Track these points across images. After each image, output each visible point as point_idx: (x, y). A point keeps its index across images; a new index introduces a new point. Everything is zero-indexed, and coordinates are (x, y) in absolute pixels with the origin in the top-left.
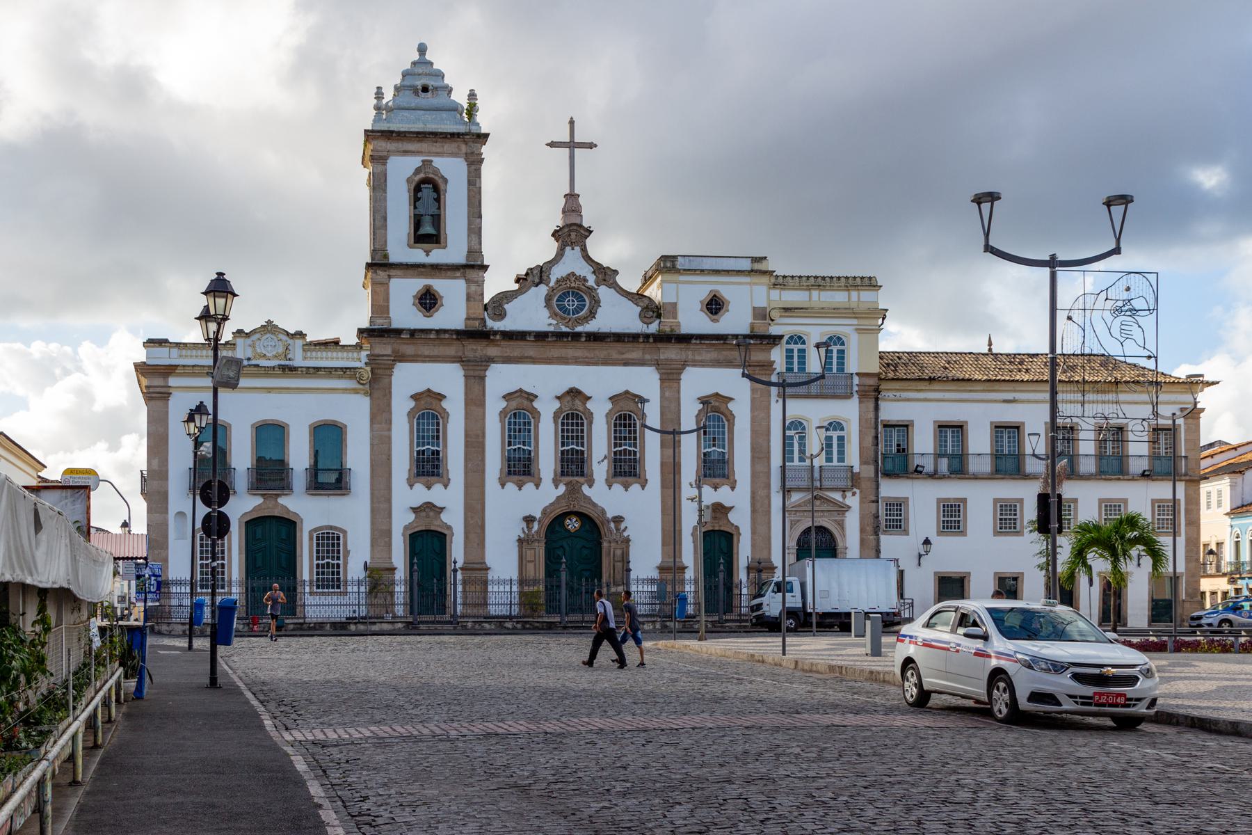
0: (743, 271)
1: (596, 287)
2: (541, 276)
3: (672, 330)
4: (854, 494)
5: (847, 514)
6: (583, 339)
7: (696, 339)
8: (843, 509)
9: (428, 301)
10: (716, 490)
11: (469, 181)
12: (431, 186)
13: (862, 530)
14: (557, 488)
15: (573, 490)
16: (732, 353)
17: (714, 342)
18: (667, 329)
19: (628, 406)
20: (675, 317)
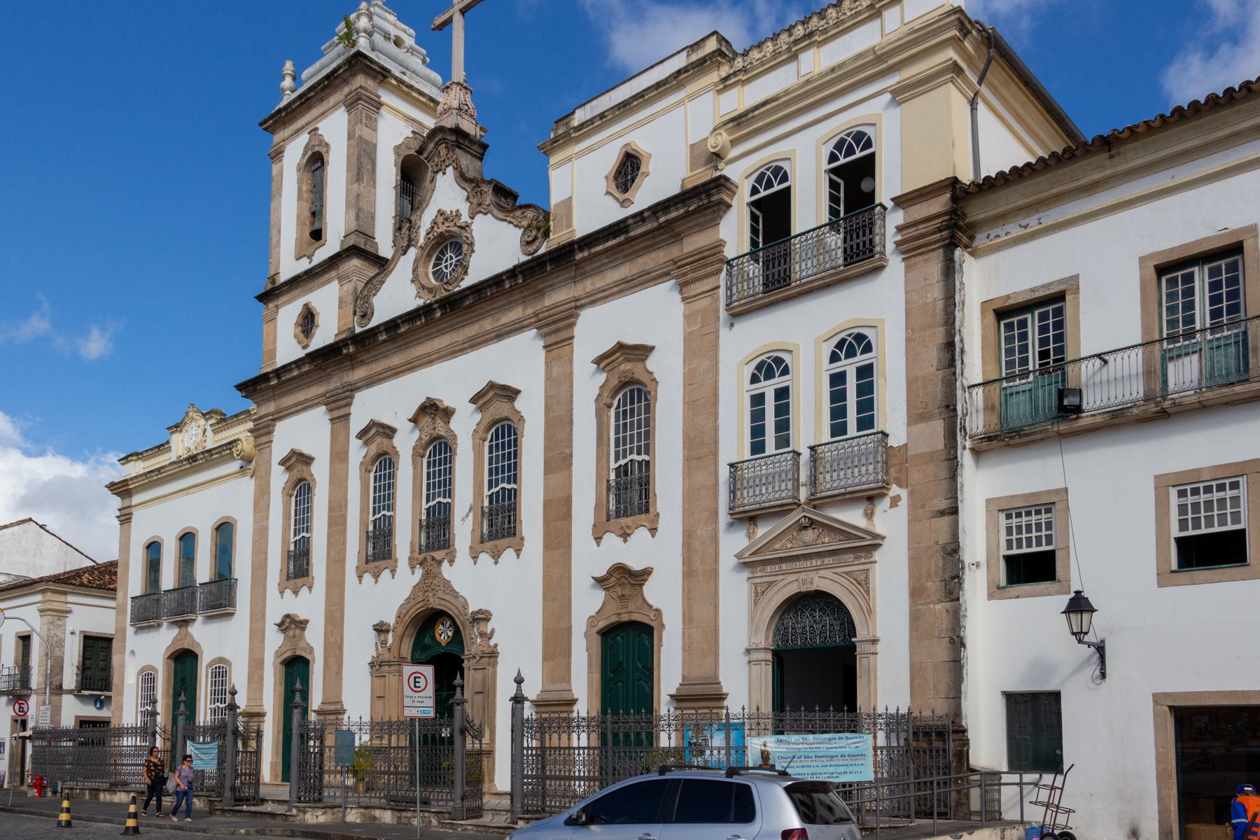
1: (470, 221)
2: (409, 235)
4: (895, 502)
5: (877, 555)
7: (581, 250)
8: (868, 545)
9: (308, 320)
10: (625, 541)
13: (916, 593)
14: (413, 573)
15: (431, 579)
16: (654, 255)
17: (610, 243)
19: (499, 409)
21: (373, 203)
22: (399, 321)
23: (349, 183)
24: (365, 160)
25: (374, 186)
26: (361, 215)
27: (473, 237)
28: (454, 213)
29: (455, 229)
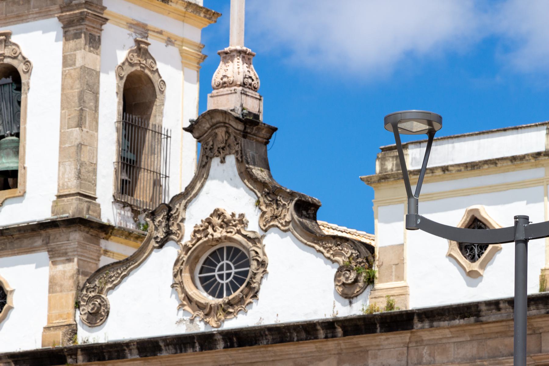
0: (522, 158)
3: (390, 306)
6: (221, 345)
11: (65, 58)
12: (10, 80)
18: (381, 307)
20: (400, 277)
21: (94, 152)
22: (162, 344)
23: (64, 124)
24: (88, 96)
25: (97, 130)
26: (83, 170)
27: (264, 254)
28: (237, 217)
29: (238, 237)
